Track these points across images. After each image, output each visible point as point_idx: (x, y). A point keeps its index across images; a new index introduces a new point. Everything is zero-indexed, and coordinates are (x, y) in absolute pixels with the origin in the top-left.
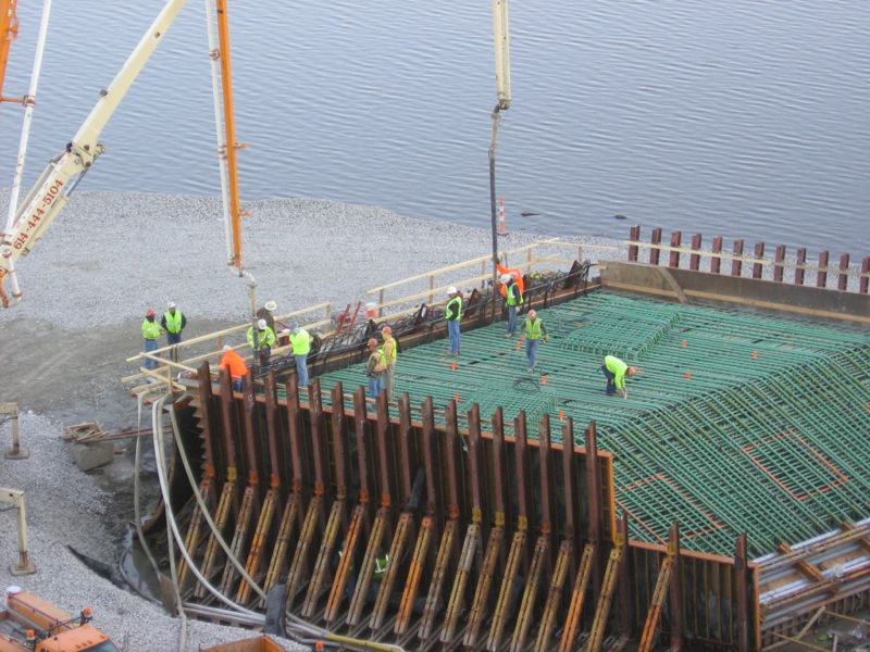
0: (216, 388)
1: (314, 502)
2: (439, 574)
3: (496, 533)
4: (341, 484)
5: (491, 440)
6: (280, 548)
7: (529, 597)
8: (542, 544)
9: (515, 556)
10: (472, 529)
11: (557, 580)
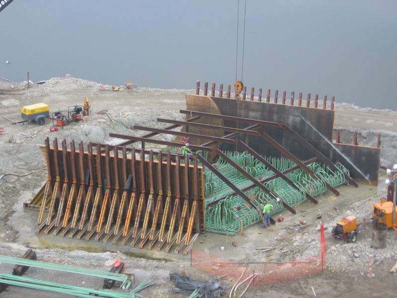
0: (52, 148)
1: (90, 189)
2: (139, 214)
3: (159, 198)
4: (99, 181)
6: (78, 206)
7: (173, 221)
8: (177, 201)
10: (150, 197)
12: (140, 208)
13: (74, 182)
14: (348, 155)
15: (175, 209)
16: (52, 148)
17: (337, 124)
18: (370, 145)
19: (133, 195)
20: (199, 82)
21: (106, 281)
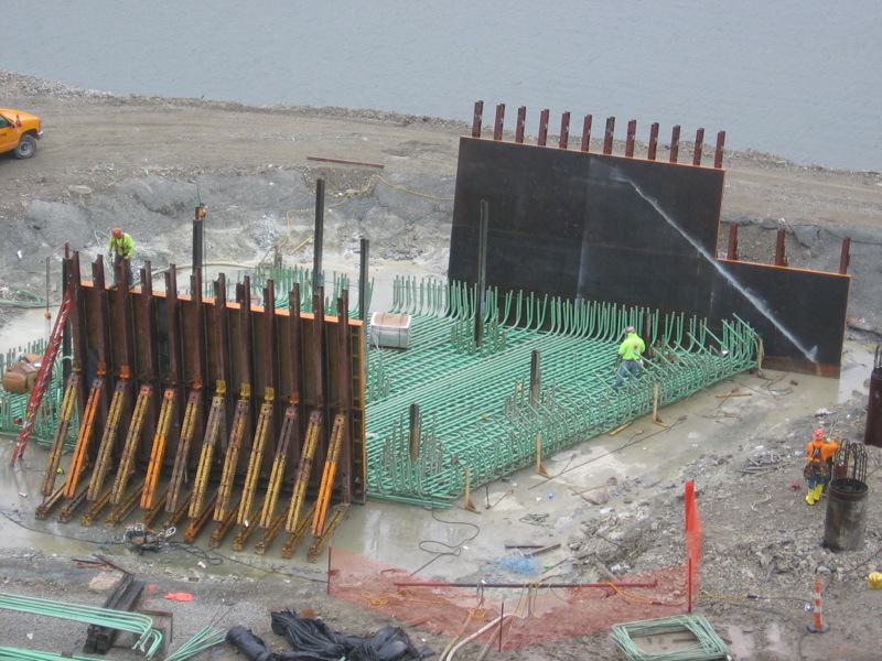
3: (242, 404)
5: (359, 327)
7: (278, 469)
8: (291, 413)
9: (263, 427)
10: (217, 401)
11: (309, 450)
12: (187, 430)
13: (125, 375)
14: (761, 293)
15: (286, 434)
16: (87, 281)
17: (729, 208)
18: (822, 265)
19: (169, 394)
20: (547, 111)
21: (93, 629)
